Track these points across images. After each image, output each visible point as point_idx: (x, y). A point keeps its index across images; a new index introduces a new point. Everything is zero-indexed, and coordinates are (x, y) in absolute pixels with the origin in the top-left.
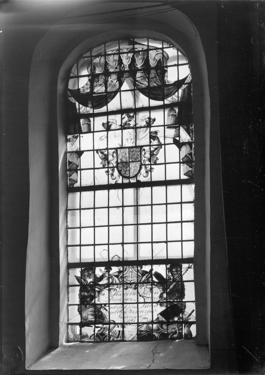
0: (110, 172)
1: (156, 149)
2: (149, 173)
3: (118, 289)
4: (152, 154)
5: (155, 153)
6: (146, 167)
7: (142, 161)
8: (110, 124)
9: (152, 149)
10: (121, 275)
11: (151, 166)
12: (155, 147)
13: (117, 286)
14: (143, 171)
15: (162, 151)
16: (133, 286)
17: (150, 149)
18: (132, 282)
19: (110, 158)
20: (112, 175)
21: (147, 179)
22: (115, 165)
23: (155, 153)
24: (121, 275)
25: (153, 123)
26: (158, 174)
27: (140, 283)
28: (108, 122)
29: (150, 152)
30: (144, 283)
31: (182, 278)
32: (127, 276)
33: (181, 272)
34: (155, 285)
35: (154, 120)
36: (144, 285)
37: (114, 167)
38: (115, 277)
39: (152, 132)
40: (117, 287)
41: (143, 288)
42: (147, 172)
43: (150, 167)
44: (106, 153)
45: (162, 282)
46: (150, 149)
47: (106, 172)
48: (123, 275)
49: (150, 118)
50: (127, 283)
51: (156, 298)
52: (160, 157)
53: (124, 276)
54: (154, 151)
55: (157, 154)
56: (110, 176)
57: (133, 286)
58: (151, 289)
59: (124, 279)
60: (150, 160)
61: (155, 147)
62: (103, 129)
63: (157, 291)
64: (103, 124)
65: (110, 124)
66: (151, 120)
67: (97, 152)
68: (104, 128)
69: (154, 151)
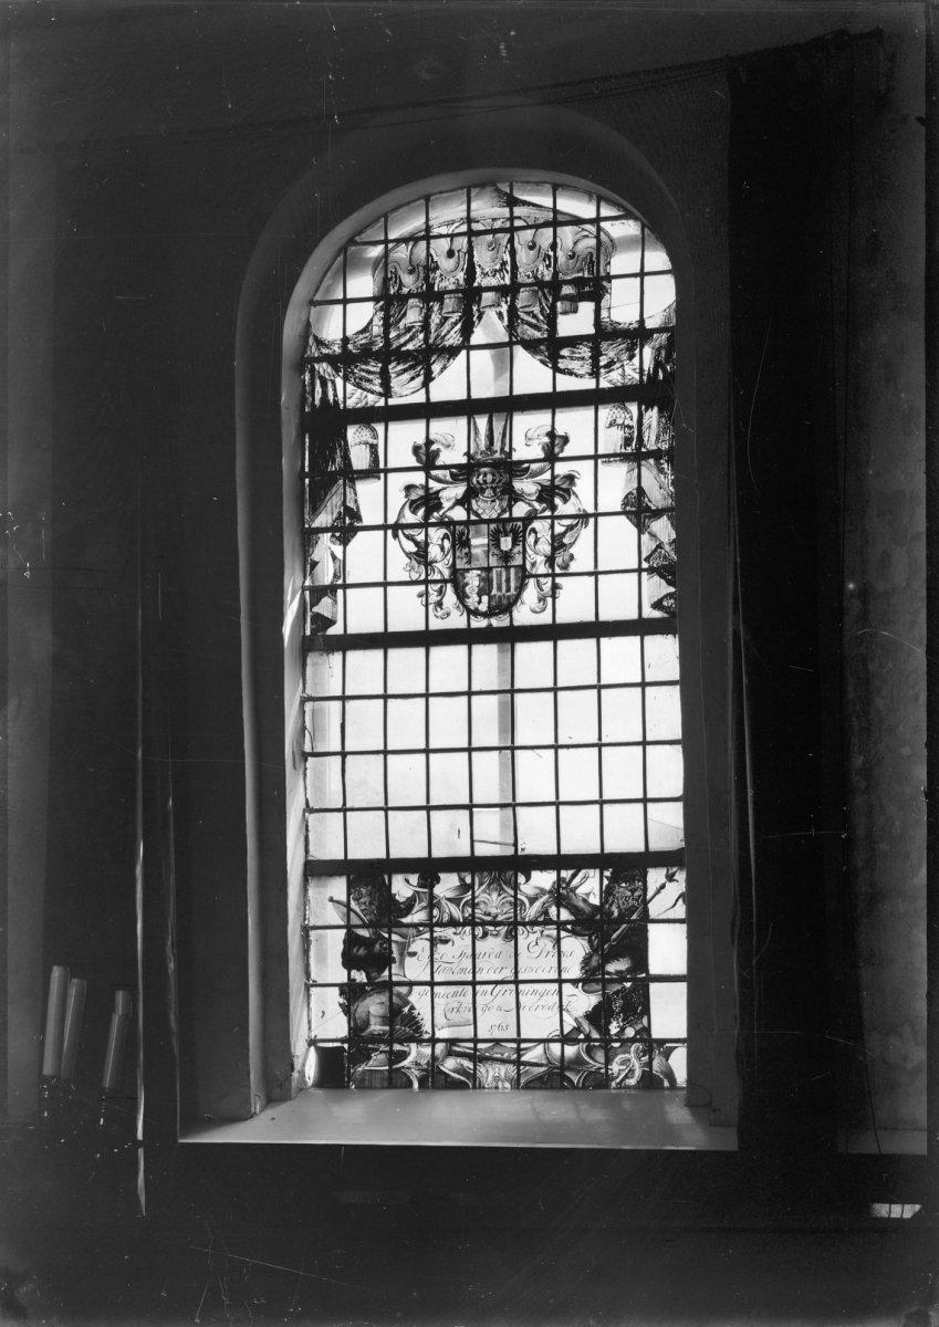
0: (434, 598)
1: (570, 528)
2: (550, 600)
3: (455, 938)
4: (558, 544)
5: (566, 541)
6: (538, 581)
7: (528, 566)
8: (434, 447)
9: (559, 529)
10: (468, 896)
11: (553, 581)
12: (568, 522)
13: (454, 930)
14: (531, 593)
15: (586, 534)
16: (503, 930)
17: (552, 527)
18: (500, 918)
19: (434, 552)
20: (439, 604)
21: (545, 618)
22: (447, 574)
23: (566, 541)
24: (468, 896)
25: (562, 451)
26: (574, 603)
27: (524, 924)
28: (429, 442)
29: (553, 536)
30: (534, 923)
31: (646, 911)
32: (484, 902)
33: (645, 889)
34: (567, 930)
35: (566, 440)
36: (536, 928)
37: (444, 581)
38: (449, 903)
39: (558, 476)
40: (455, 934)
41: (533, 937)
42: (542, 599)
43: (549, 584)
44: (421, 538)
45: (588, 923)
46: (552, 527)
47: (420, 596)
48: (473, 898)
49: (552, 434)
50: (483, 923)
51: (573, 970)
53: (476, 901)
54: (563, 535)
55: (572, 544)
56: (431, 607)
57: (503, 930)
58: (558, 941)
59: (476, 911)
60: (550, 560)
61: (568, 522)
62: (413, 462)
63: (576, 949)
64: (416, 450)
65: (434, 447)
66: (557, 442)
67: (395, 536)
68: (419, 460)
69: (563, 535)
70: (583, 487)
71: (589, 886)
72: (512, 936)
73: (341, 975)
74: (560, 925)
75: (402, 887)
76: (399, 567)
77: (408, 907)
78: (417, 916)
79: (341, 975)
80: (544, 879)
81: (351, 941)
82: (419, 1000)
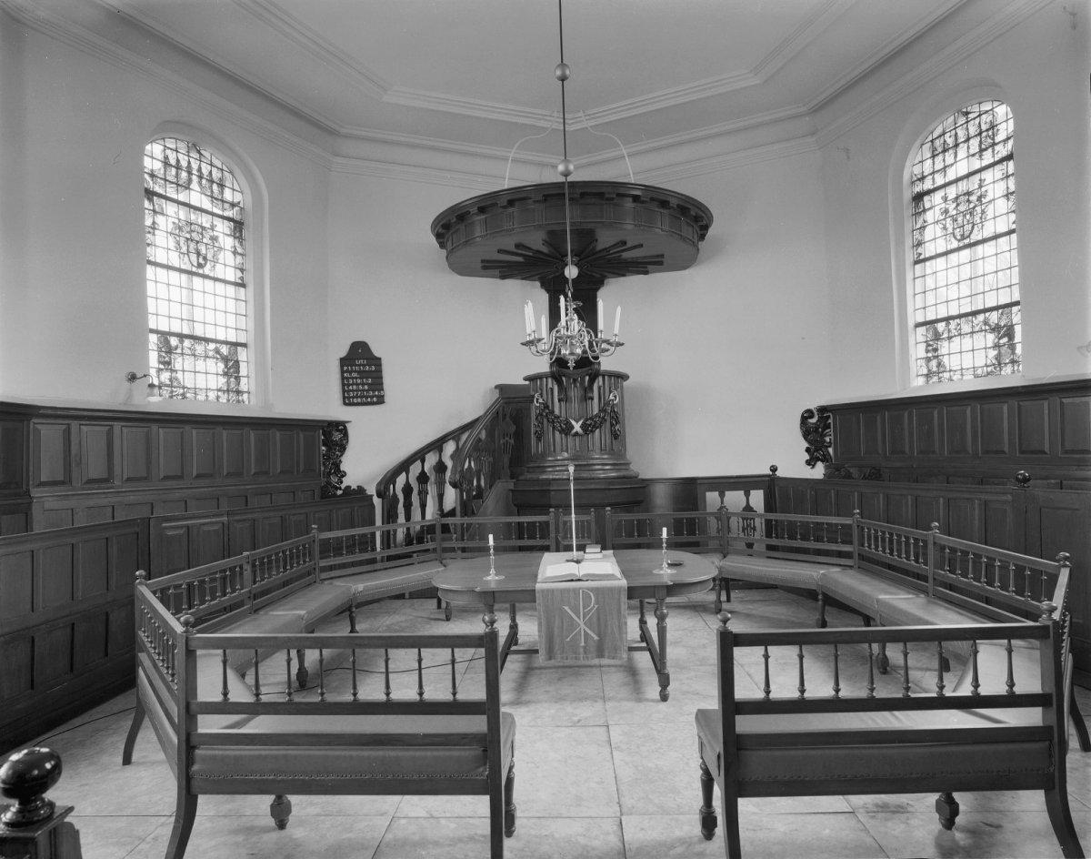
14: (208, 266)
15: (222, 253)
45: (225, 360)
52: (221, 256)
70: (221, 239)
71: (224, 350)
72: (205, 360)
73: (157, 366)
74: (217, 359)
75: (174, 341)
76: (172, 244)
77: (176, 348)
78: (179, 351)
79: (157, 366)
80: (212, 346)
81: (160, 356)
82: (179, 375)
